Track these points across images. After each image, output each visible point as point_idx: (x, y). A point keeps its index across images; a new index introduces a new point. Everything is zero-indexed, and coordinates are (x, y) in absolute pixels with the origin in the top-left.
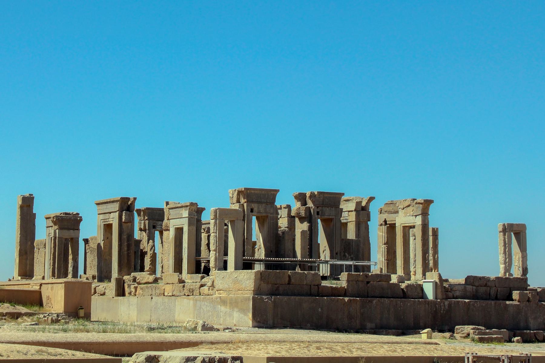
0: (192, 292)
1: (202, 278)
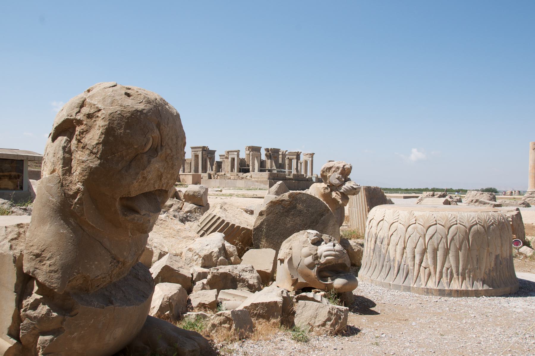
0: (243, 178)
1: (243, 174)
